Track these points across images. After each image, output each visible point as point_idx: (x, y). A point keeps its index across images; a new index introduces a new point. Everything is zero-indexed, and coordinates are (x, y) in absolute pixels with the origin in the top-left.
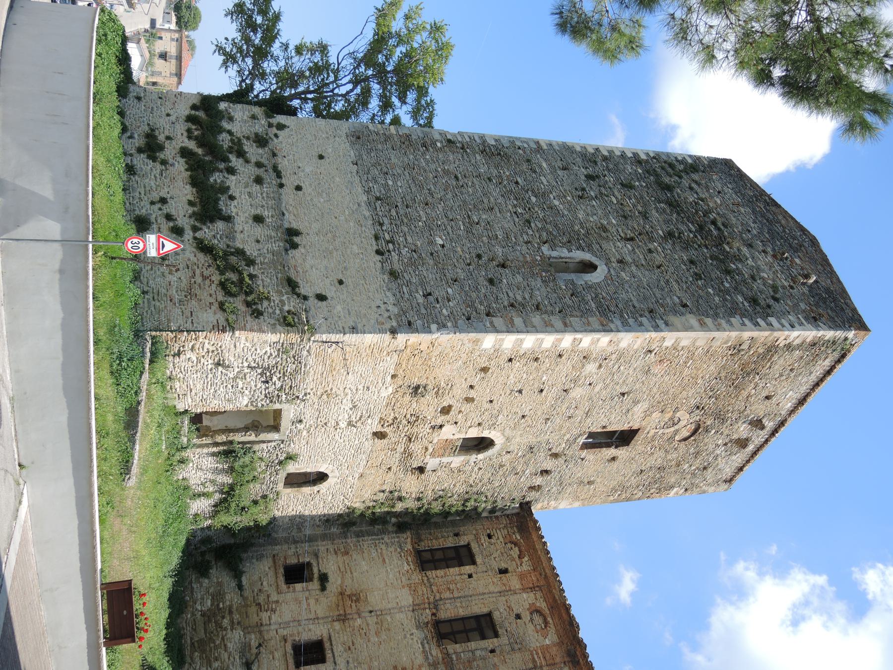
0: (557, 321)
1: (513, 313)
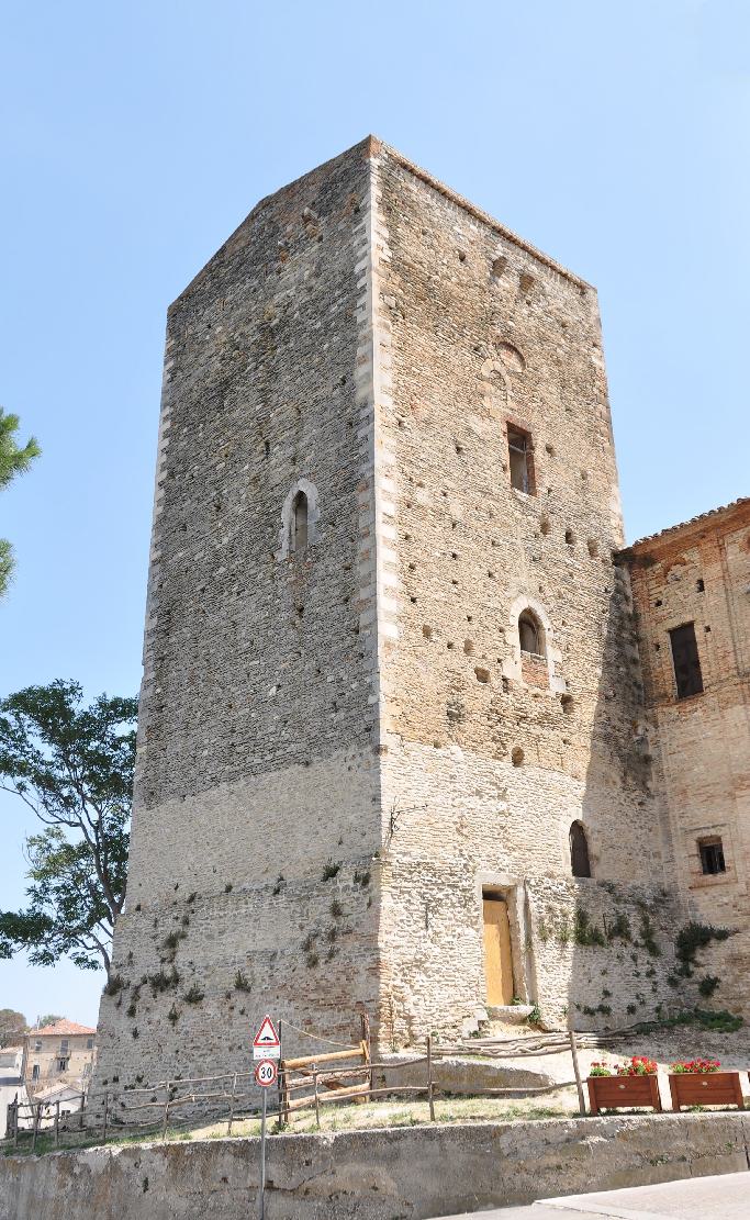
0: (363, 545)
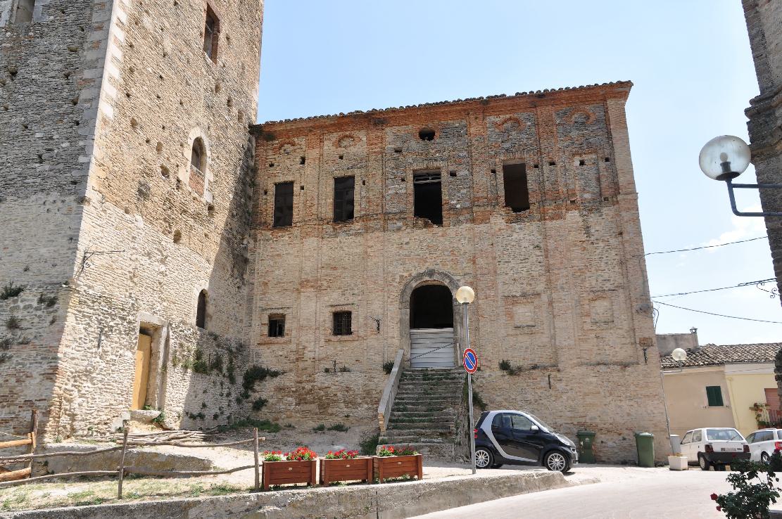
1: (75, 78)
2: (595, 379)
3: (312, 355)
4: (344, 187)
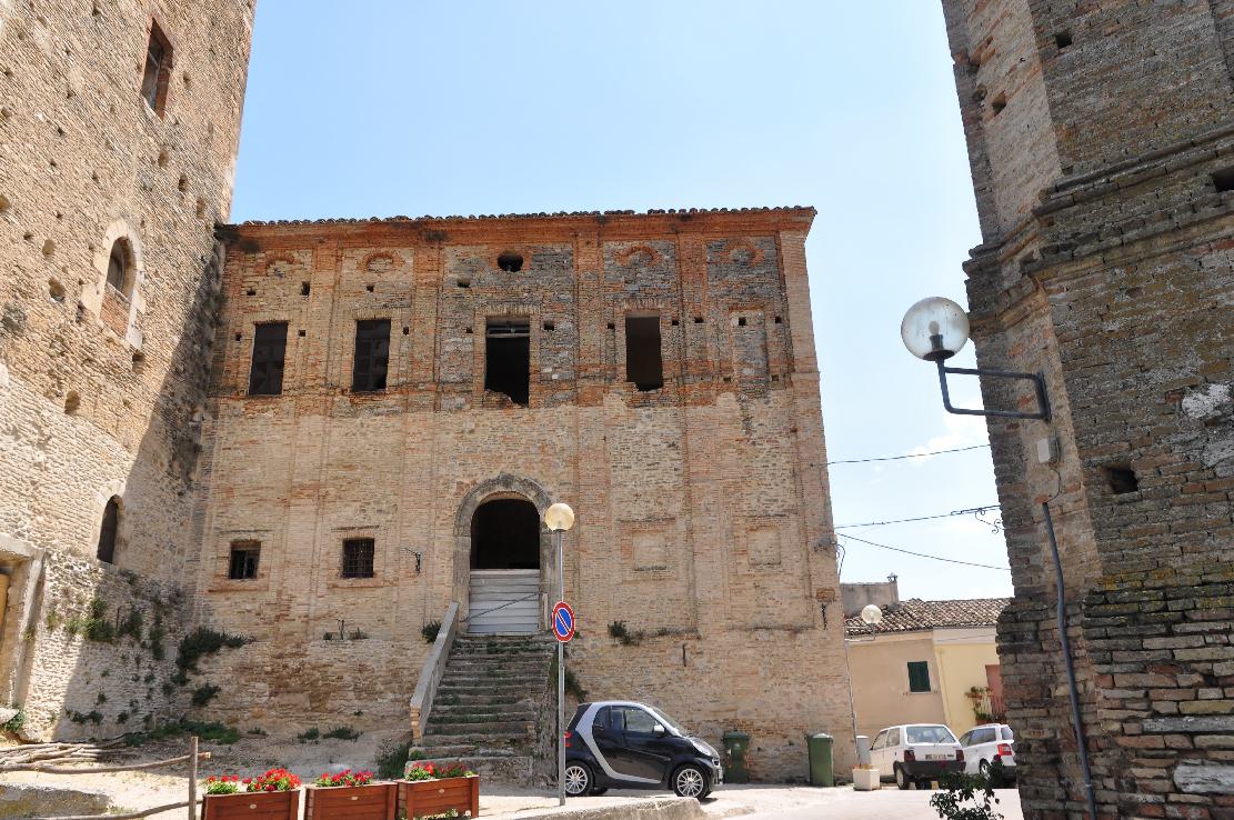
2: (750, 652)
3: (302, 610)
4: (372, 339)
